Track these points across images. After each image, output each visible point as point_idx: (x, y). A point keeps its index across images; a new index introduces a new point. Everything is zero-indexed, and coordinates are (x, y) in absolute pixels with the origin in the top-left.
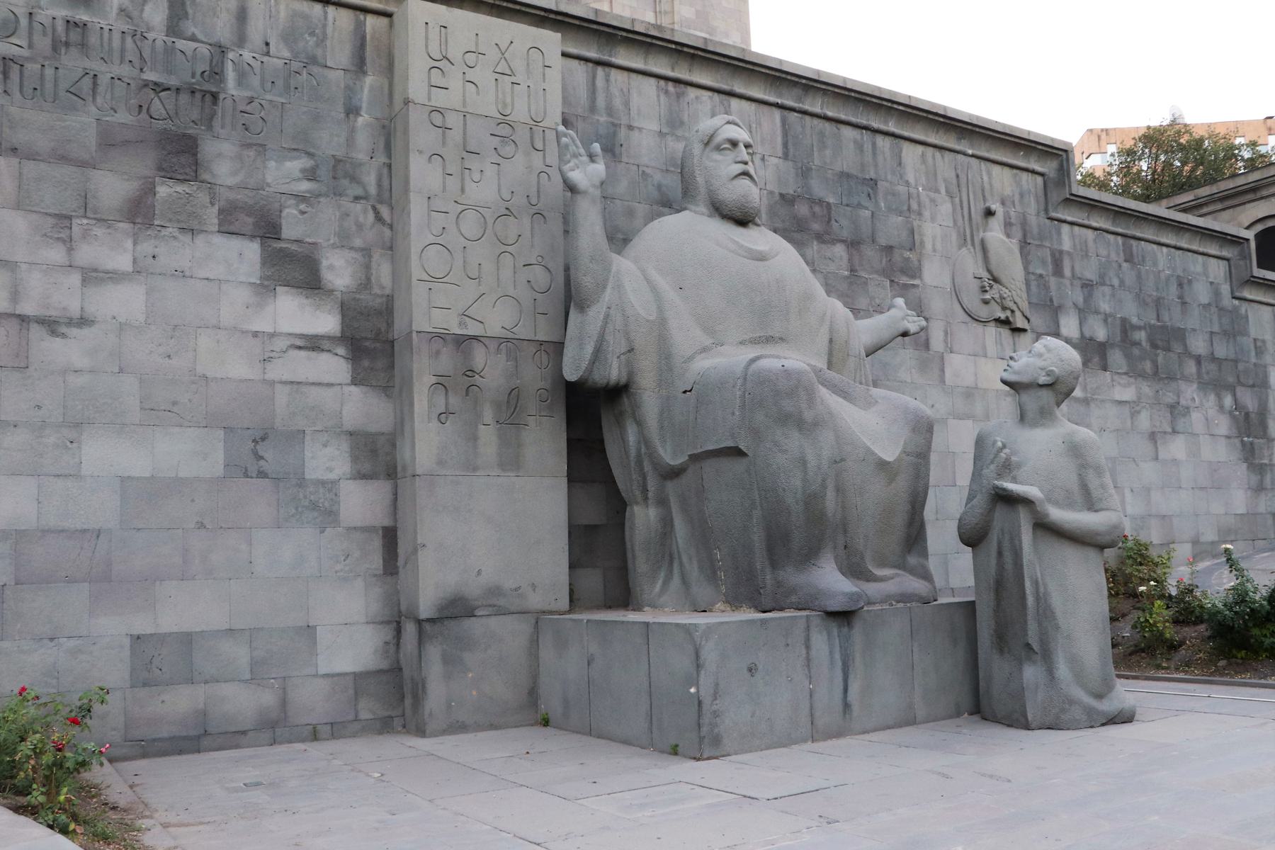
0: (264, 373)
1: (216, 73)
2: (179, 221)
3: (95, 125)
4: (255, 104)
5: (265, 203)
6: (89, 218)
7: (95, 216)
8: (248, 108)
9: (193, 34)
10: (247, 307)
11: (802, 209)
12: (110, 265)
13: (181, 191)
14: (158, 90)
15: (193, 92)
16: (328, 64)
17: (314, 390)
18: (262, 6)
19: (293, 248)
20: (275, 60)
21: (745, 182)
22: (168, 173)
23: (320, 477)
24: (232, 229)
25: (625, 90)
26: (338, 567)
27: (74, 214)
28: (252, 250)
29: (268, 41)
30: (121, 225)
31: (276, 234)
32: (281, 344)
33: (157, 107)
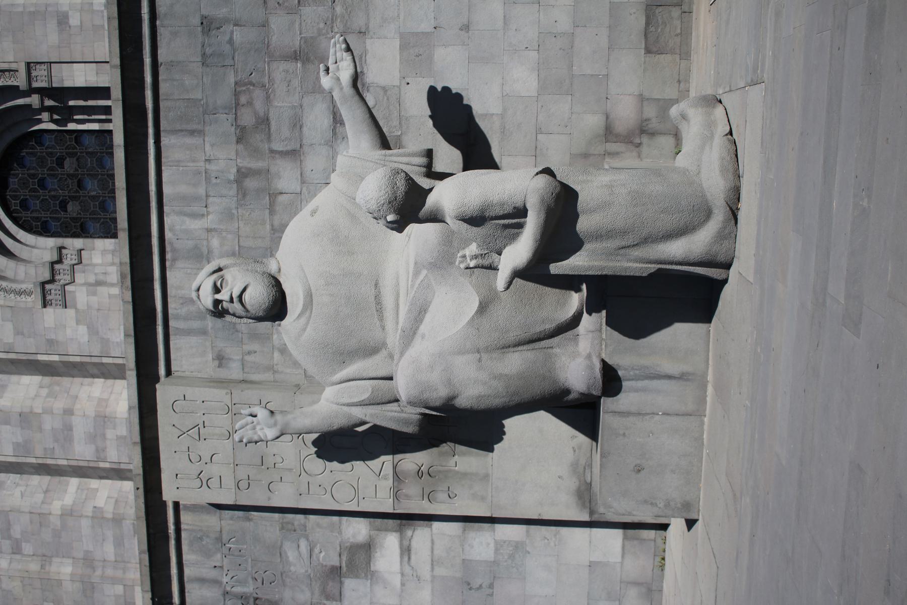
0: (427, 581)
4: (256, 576)
5: (318, 574)
8: (260, 581)
11: (247, 118)
17: (436, 552)
18: (192, 569)
19: (345, 559)
20: (224, 563)
21: (247, 297)
23: (493, 552)
24: (337, 594)
25: (181, 301)
26: (552, 544)
28: (350, 584)
31: (337, 569)
32: (407, 570)
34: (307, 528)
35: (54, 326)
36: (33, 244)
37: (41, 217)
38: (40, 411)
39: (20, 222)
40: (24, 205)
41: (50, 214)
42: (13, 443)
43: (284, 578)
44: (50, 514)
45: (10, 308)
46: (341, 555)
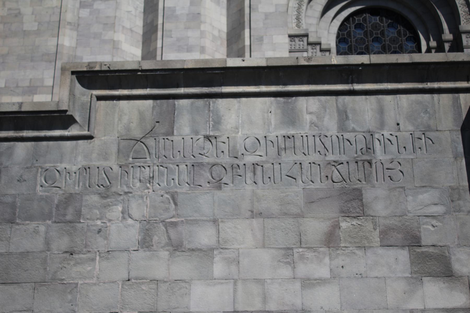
1: (369, 149)
2: (355, 242)
3: (302, 192)
4: (395, 163)
5: (409, 223)
6: (304, 248)
7: (306, 246)
8: (390, 166)
9: (353, 128)
10: (405, 293)
12: (317, 276)
13: (355, 224)
14: (336, 164)
15: (357, 162)
16: (438, 129)
18: (392, 103)
19: (430, 251)
20: (404, 133)
22: (346, 214)
24: (389, 243)
27: (294, 246)
29: (399, 123)
30: (321, 249)
31: (418, 243)
33: (336, 175)
34: (457, 213)
35: (274, 42)
36: (330, 31)
37: (351, 38)
38: (203, 27)
39: (345, 23)
40: (359, 26)
41: (354, 45)
42: (175, 7)
43: (398, 190)
44: (115, 32)
45: (286, 11)
46: (433, 247)
